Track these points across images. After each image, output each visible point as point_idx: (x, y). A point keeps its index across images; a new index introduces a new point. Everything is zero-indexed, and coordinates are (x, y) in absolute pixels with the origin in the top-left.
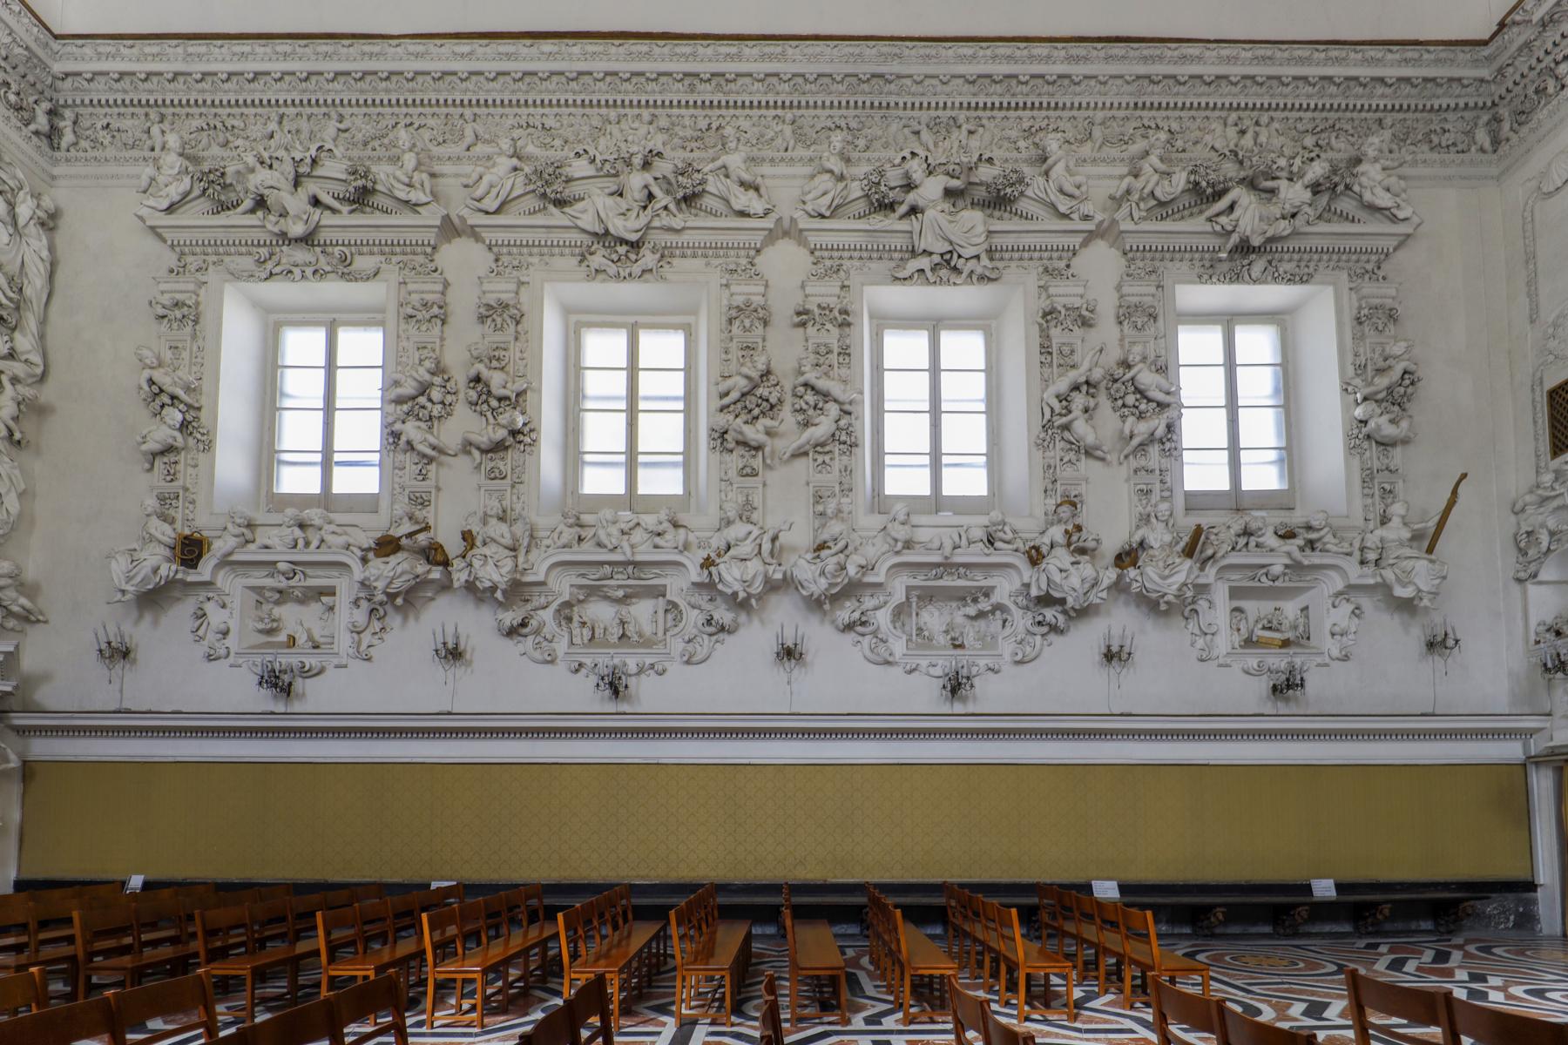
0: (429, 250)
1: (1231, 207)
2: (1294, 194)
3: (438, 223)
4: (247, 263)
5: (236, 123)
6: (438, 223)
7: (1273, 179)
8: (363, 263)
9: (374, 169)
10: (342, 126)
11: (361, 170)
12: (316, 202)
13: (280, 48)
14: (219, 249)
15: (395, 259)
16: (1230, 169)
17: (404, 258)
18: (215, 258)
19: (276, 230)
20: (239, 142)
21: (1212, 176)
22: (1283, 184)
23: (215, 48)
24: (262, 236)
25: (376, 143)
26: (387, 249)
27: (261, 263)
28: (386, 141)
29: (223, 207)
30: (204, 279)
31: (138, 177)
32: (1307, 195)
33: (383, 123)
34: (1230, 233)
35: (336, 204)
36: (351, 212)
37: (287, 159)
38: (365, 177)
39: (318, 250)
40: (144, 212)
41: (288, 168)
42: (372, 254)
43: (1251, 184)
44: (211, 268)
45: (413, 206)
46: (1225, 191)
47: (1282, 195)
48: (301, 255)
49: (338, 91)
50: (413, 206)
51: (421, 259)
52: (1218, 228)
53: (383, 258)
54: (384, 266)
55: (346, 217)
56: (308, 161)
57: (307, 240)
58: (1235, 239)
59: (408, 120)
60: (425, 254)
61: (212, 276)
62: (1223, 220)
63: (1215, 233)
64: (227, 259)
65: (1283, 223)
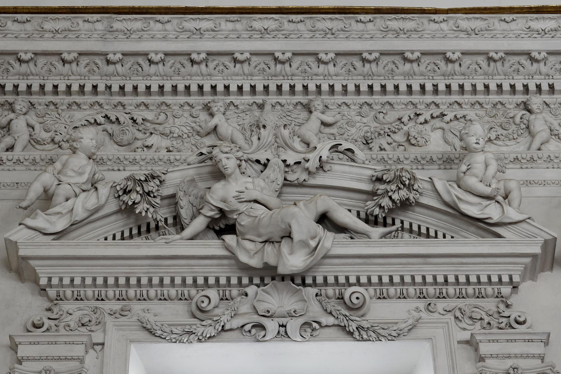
0: (506, 290)
3: (537, 250)
4: (174, 313)
5: (150, 116)
6: (537, 250)
8: (379, 311)
9: (419, 174)
10: (328, 118)
11: (406, 177)
12: (324, 219)
13: (257, 25)
14: (127, 291)
15: (441, 305)
17: (460, 303)
18: (117, 306)
19: (255, 262)
20: (153, 140)
23: (154, 25)
24: (222, 272)
25: (383, 141)
26: (432, 291)
27: (199, 313)
28: (399, 137)
29: (147, 229)
30: (97, 337)
31: (28, 185)
33: (392, 116)
35: (361, 225)
36: (384, 236)
37: (275, 161)
38: (410, 187)
39: (313, 291)
40: (19, 235)
41: (275, 173)
42: (403, 296)
44: (109, 321)
45: (484, 226)
48: (276, 300)
49: (321, 76)
50: (484, 226)
51: (490, 305)
53: (421, 304)
54: (424, 315)
55: (376, 242)
56: (313, 164)
57: (298, 280)
59: (437, 113)
60: (499, 295)
61: (112, 334)
64: (137, 307)
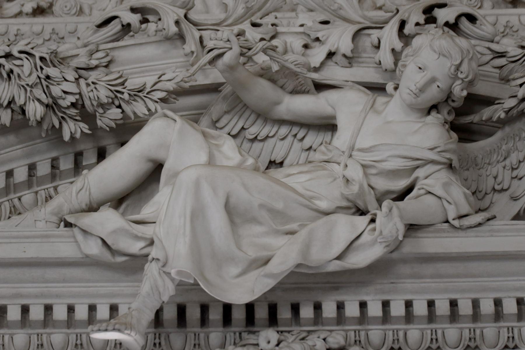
1: (154, 173)
2: (386, 132)
7: (320, 87)
16: (148, 63)
21: (65, 88)
22: (346, 105)
32: (430, 136)
34: (135, 264)
43: (205, 101)
46: (126, 130)
47: (342, 139)
52: (93, 248)
58: (153, 290)
62: (108, 221)
63: (88, 262)
65: (346, 227)
